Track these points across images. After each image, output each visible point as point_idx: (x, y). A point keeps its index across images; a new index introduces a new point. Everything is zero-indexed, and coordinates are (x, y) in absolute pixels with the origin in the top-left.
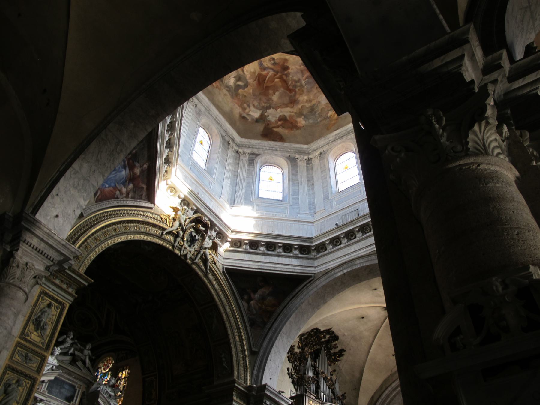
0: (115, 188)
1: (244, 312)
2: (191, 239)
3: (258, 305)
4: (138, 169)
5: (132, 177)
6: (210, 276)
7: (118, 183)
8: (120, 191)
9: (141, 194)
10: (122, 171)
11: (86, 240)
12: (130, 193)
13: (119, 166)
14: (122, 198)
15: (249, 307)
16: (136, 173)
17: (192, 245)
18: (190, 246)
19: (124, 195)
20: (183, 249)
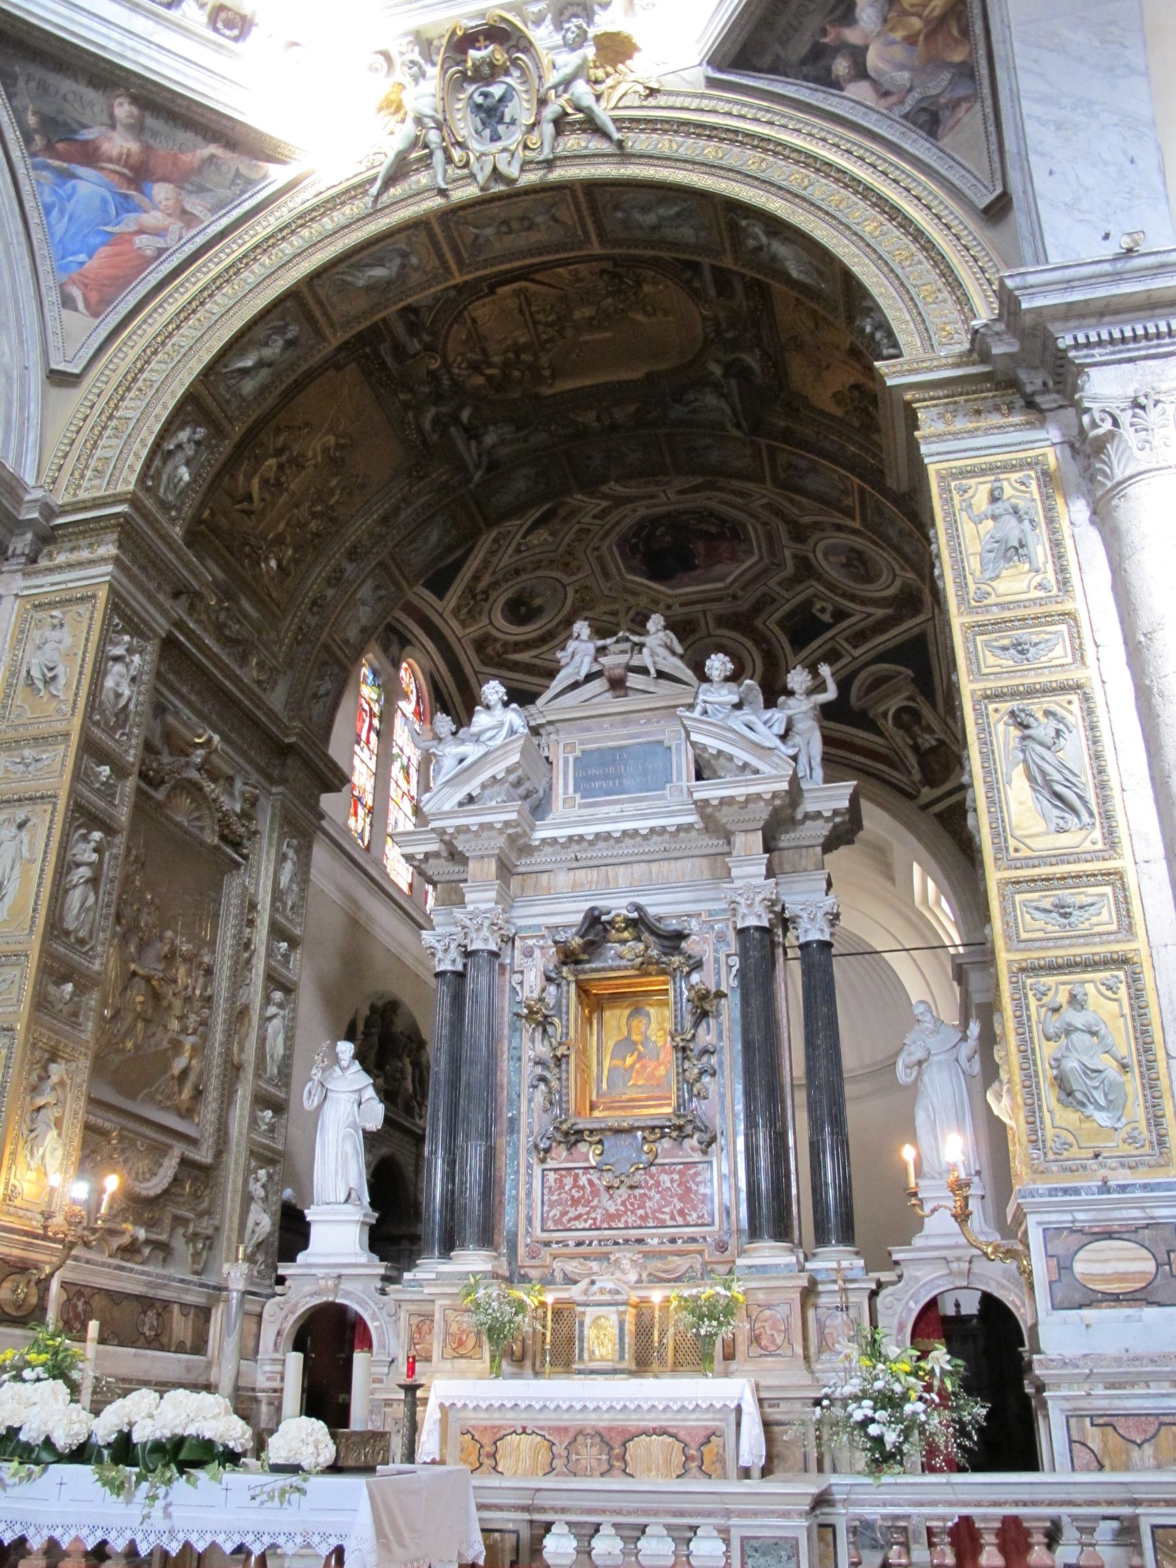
0: (113, 239)
2: (483, 115)
3: (893, 42)
4: (110, 139)
5: (126, 171)
7: (106, 224)
9: (231, 176)
10: (74, 188)
12: (188, 208)
13: (47, 190)
14: (181, 238)
15: (875, 83)
16: (120, 155)
17: (501, 129)
18: (495, 138)
19: (176, 226)
20: (475, 166)
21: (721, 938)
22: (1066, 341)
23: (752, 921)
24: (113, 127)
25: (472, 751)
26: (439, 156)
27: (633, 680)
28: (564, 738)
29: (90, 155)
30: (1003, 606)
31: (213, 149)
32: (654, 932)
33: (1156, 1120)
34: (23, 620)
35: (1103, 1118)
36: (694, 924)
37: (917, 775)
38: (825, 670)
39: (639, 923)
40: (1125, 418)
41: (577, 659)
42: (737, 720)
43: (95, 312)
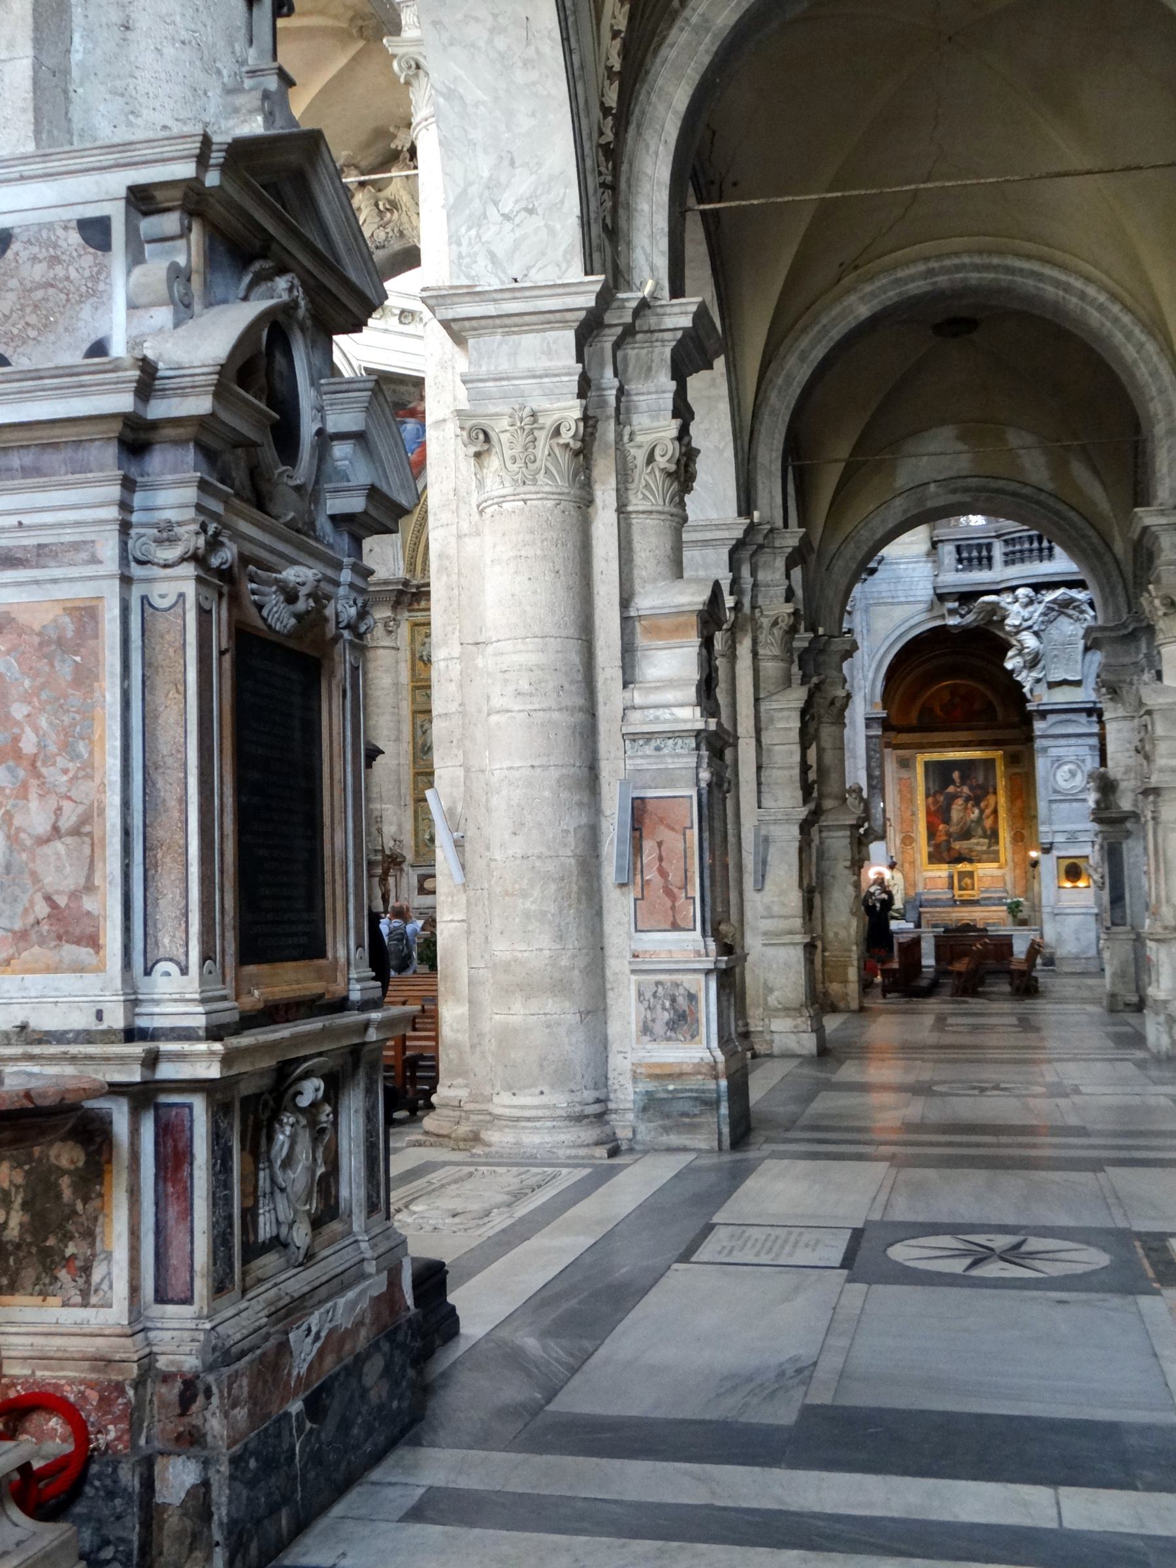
34: (412, 631)
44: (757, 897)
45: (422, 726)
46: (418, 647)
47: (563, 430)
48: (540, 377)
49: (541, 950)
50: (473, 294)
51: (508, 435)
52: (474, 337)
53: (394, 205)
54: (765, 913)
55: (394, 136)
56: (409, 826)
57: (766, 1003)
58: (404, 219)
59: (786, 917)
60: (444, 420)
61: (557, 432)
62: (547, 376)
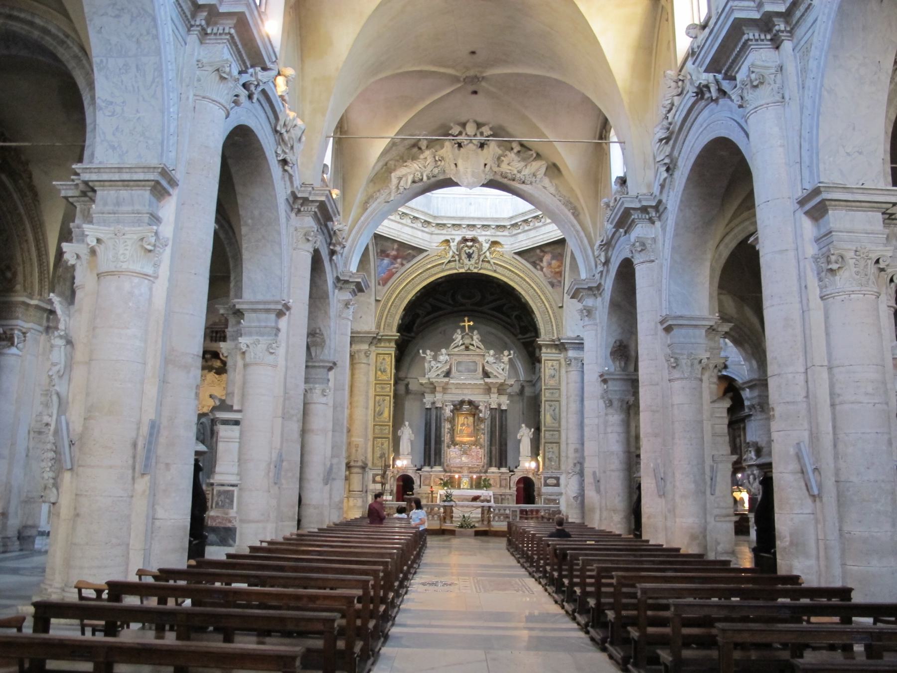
0: (389, 270)
1: (542, 279)
6: (499, 269)
8: (394, 268)
11: (389, 312)
15: (544, 274)
21: (486, 407)
22: (566, 346)
23: (494, 407)
24: (393, 249)
25: (439, 365)
26: (457, 262)
27: (471, 347)
28: (455, 357)
29: (388, 256)
30: (551, 386)
31: (410, 251)
32: (474, 406)
33: (559, 464)
35: (553, 463)
36: (481, 404)
37: (518, 331)
38: (512, 352)
39: (470, 403)
40: (573, 360)
41: (457, 340)
42: (495, 366)
43: (384, 285)
44: (712, 498)
45: (379, 402)
46: (378, 364)
47: (881, 261)
48: (869, 233)
49: (886, 531)
50: (845, 189)
51: (854, 260)
52: (833, 210)
53: (442, 159)
54: (716, 505)
55: (451, 128)
56: (370, 450)
57: (716, 549)
58: (447, 165)
59: (726, 508)
60: (787, 250)
61: (877, 262)
62: (872, 233)
